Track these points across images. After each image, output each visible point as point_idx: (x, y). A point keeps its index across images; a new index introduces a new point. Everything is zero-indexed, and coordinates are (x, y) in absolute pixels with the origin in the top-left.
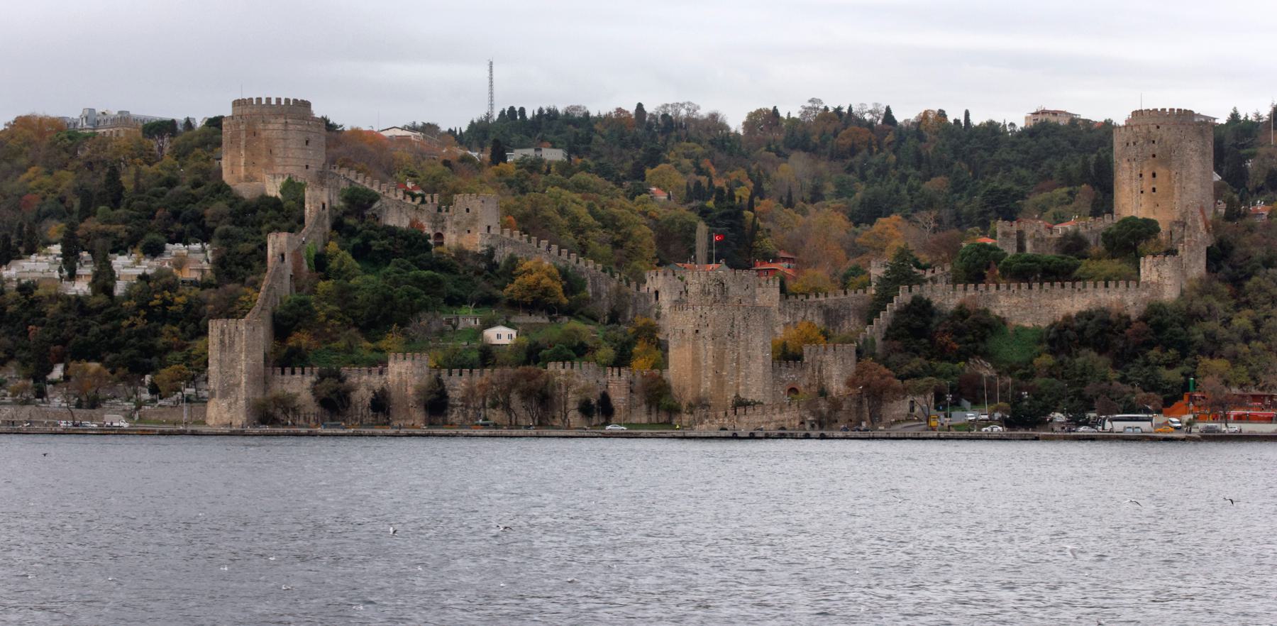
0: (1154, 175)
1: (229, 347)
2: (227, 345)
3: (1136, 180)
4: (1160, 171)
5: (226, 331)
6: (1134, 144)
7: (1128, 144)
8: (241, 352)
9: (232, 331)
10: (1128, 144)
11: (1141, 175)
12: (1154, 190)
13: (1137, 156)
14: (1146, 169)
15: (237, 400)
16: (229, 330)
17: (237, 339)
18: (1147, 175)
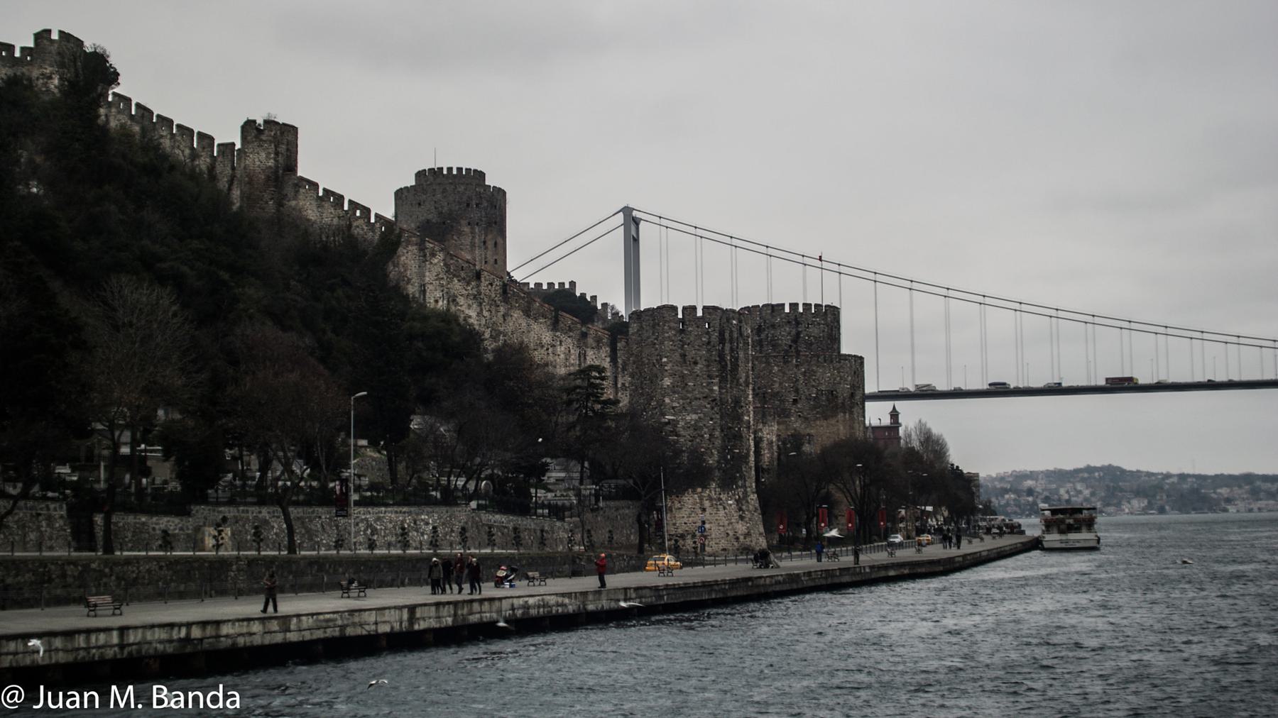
0: (496, 244)
1: (731, 371)
2: (729, 368)
3: (480, 247)
4: (500, 240)
5: (727, 335)
6: (477, 205)
7: (468, 205)
8: (748, 386)
9: (735, 335)
10: (468, 205)
11: (485, 243)
12: (496, 260)
13: (481, 220)
14: (490, 237)
15: (746, 495)
16: (731, 332)
17: (741, 354)
18: (490, 244)
